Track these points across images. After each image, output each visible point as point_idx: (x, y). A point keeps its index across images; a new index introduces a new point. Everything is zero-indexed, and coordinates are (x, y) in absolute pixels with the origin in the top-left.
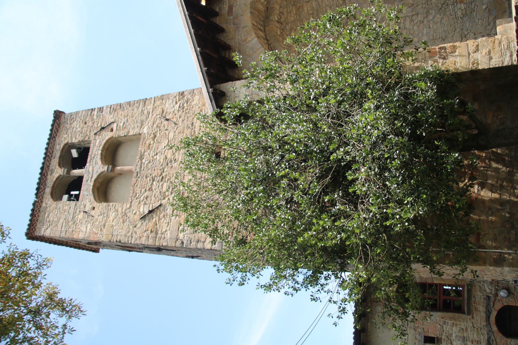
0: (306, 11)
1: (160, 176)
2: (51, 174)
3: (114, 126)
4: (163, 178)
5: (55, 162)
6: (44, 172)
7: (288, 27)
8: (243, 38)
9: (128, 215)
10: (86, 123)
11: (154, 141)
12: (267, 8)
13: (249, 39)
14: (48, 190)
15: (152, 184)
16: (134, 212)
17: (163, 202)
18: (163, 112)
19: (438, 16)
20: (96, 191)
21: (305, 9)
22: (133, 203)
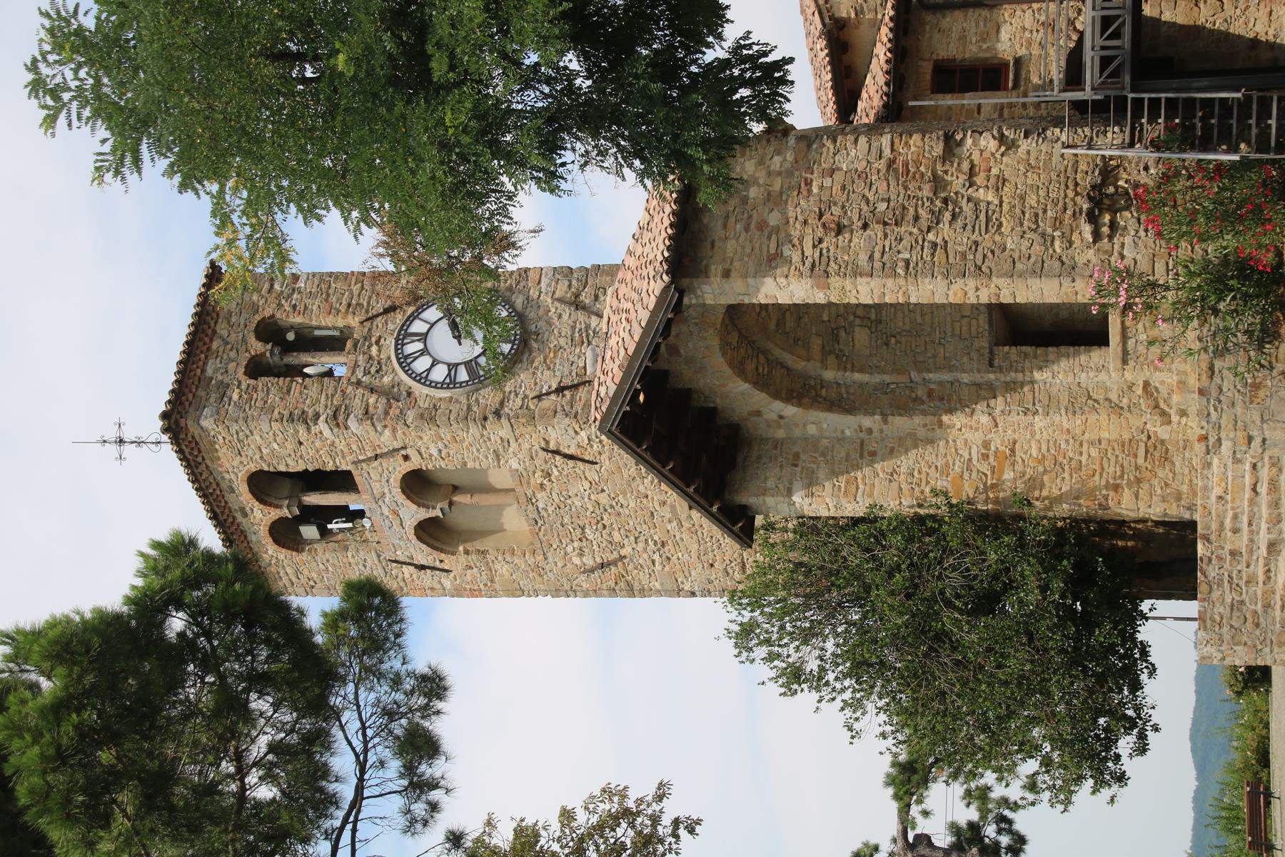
1: (598, 522)
2: (245, 515)
3: (409, 451)
4: (604, 527)
6: (222, 518)
9: (547, 568)
13: (731, 385)
16: (560, 565)
17: (623, 552)
18: (547, 442)
20: (424, 536)
22: (549, 555)
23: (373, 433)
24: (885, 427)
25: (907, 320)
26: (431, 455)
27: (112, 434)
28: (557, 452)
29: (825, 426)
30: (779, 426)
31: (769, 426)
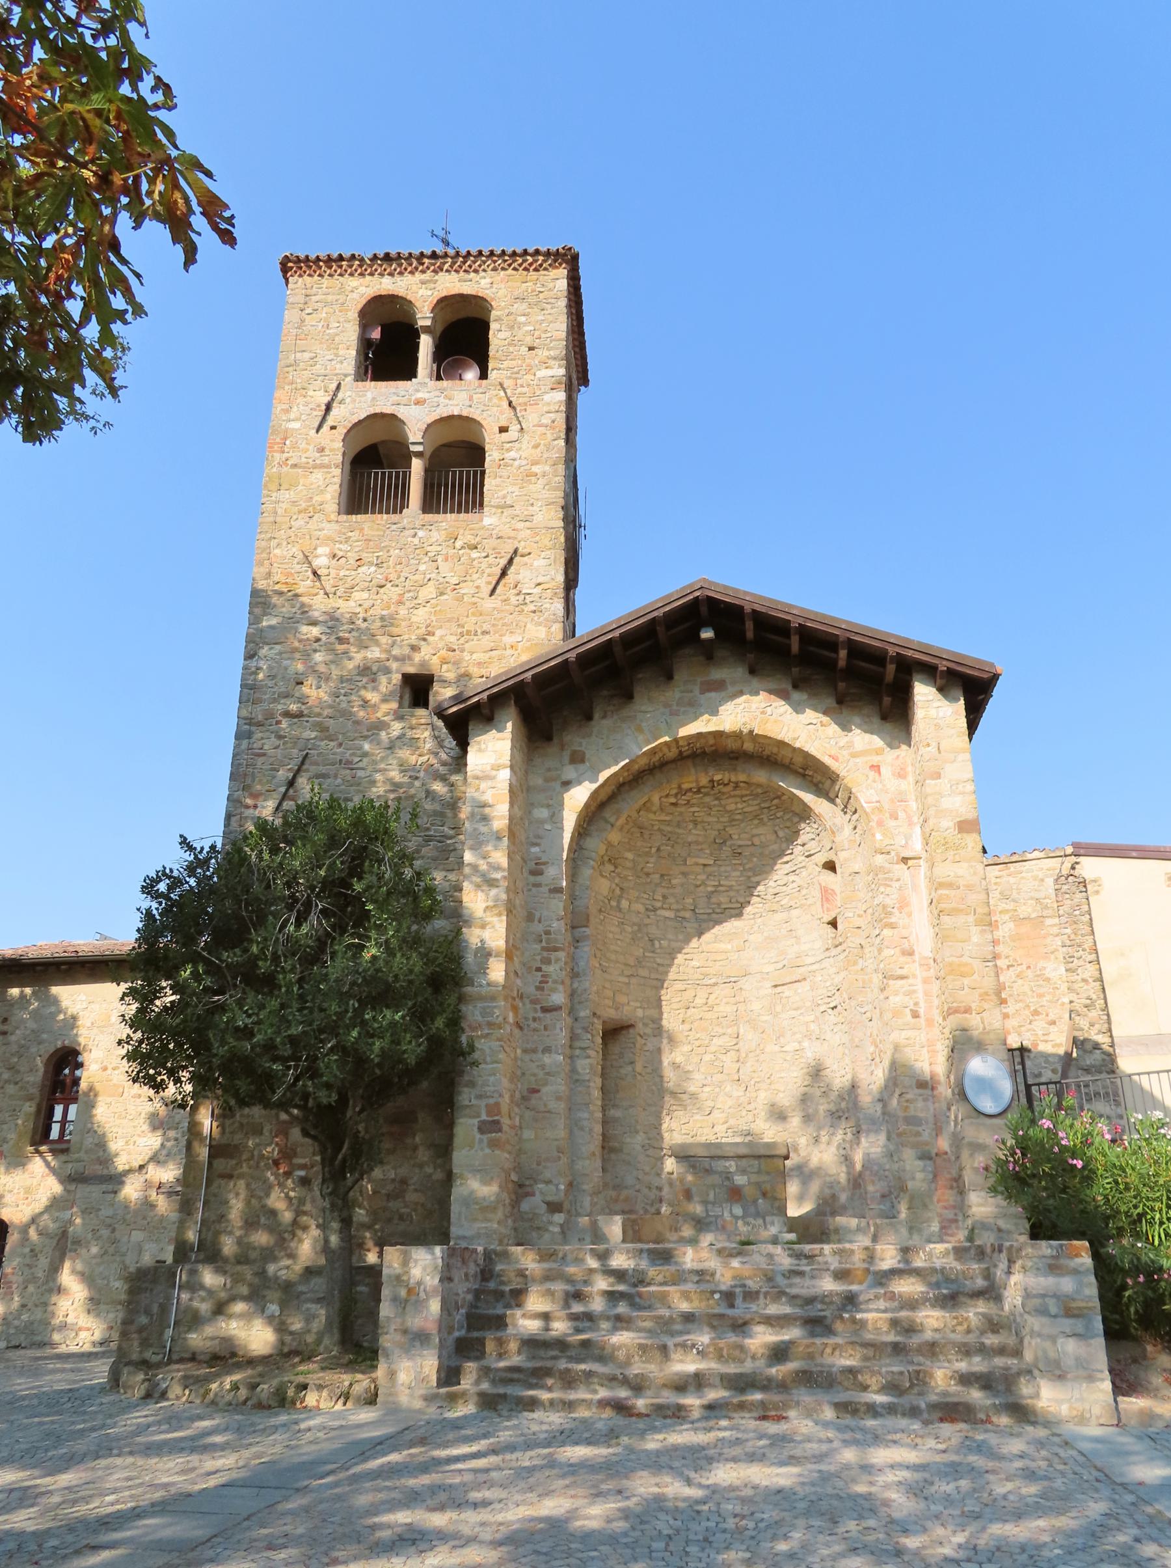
0: (755, 831)
5: (451, 283)
7: (707, 799)
8: (644, 724)
10: (531, 349)
11: (462, 547)
12: (737, 758)
14: (386, 285)
15: (371, 564)
19: (730, 1103)
21: (760, 830)
23: (546, 409)
24: (545, 889)
25: (611, 936)
26: (509, 450)
27: (450, 239)
28: (511, 561)
29: (548, 827)
30: (547, 780)
31: (549, 770)
